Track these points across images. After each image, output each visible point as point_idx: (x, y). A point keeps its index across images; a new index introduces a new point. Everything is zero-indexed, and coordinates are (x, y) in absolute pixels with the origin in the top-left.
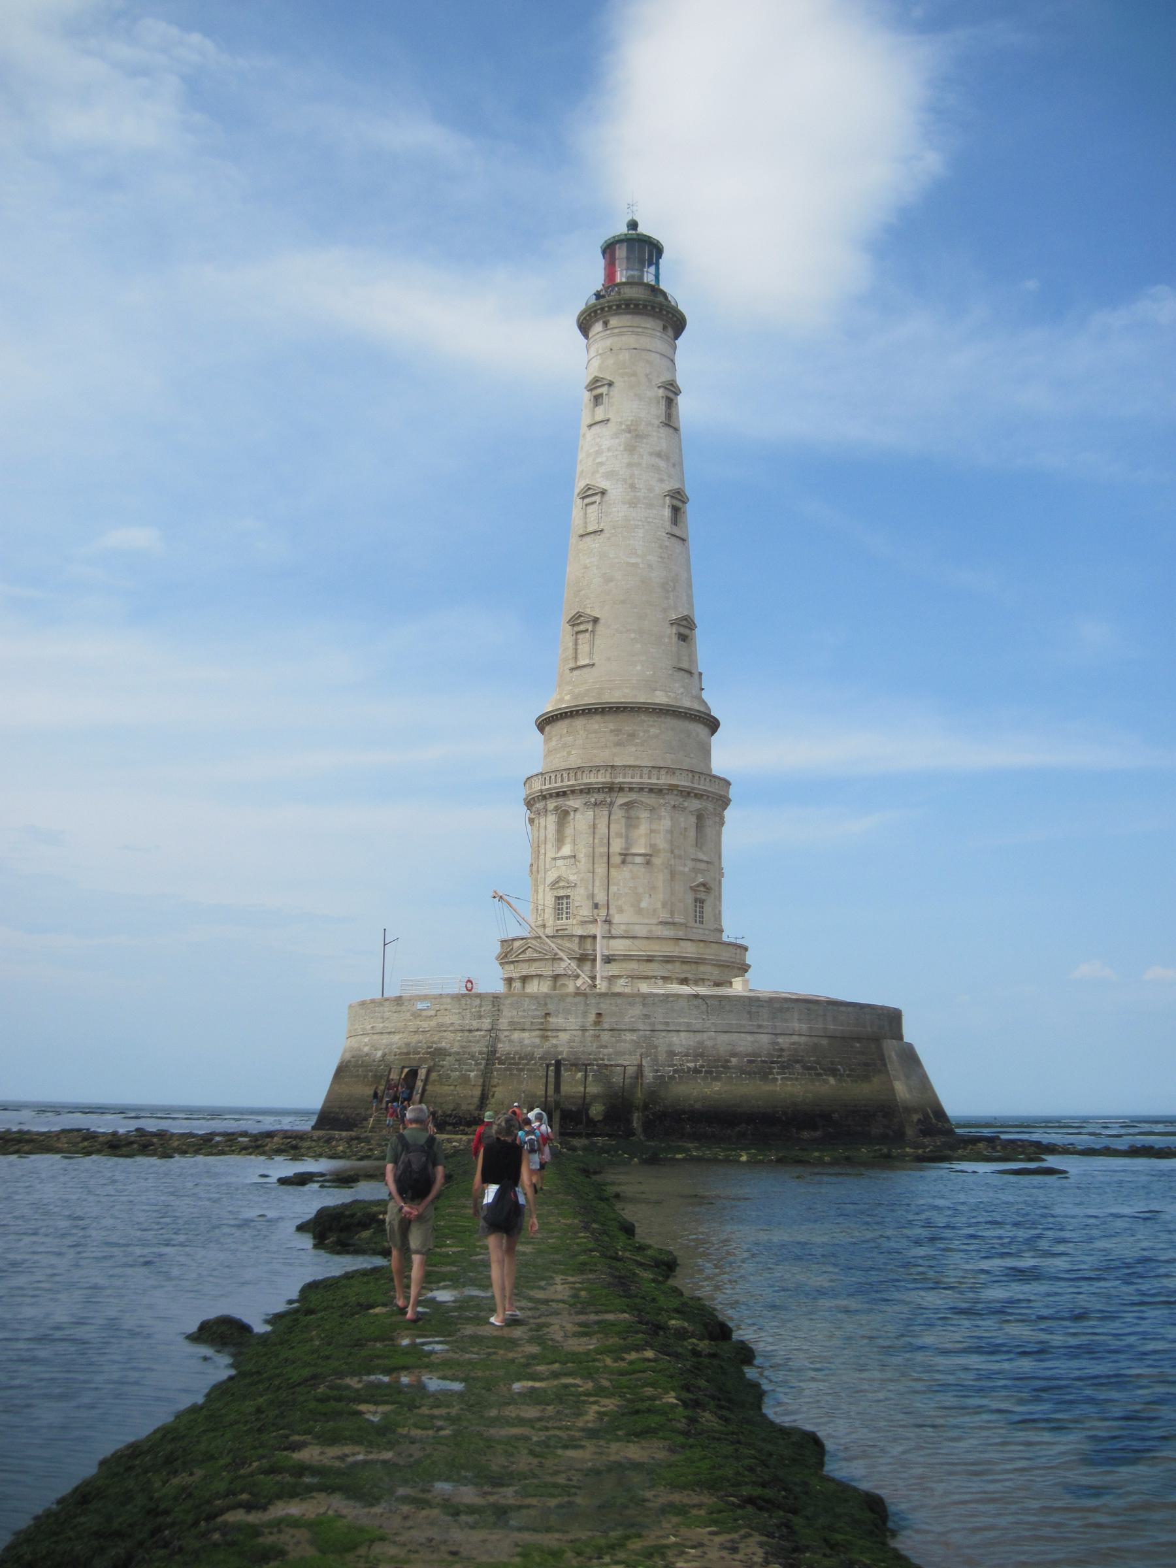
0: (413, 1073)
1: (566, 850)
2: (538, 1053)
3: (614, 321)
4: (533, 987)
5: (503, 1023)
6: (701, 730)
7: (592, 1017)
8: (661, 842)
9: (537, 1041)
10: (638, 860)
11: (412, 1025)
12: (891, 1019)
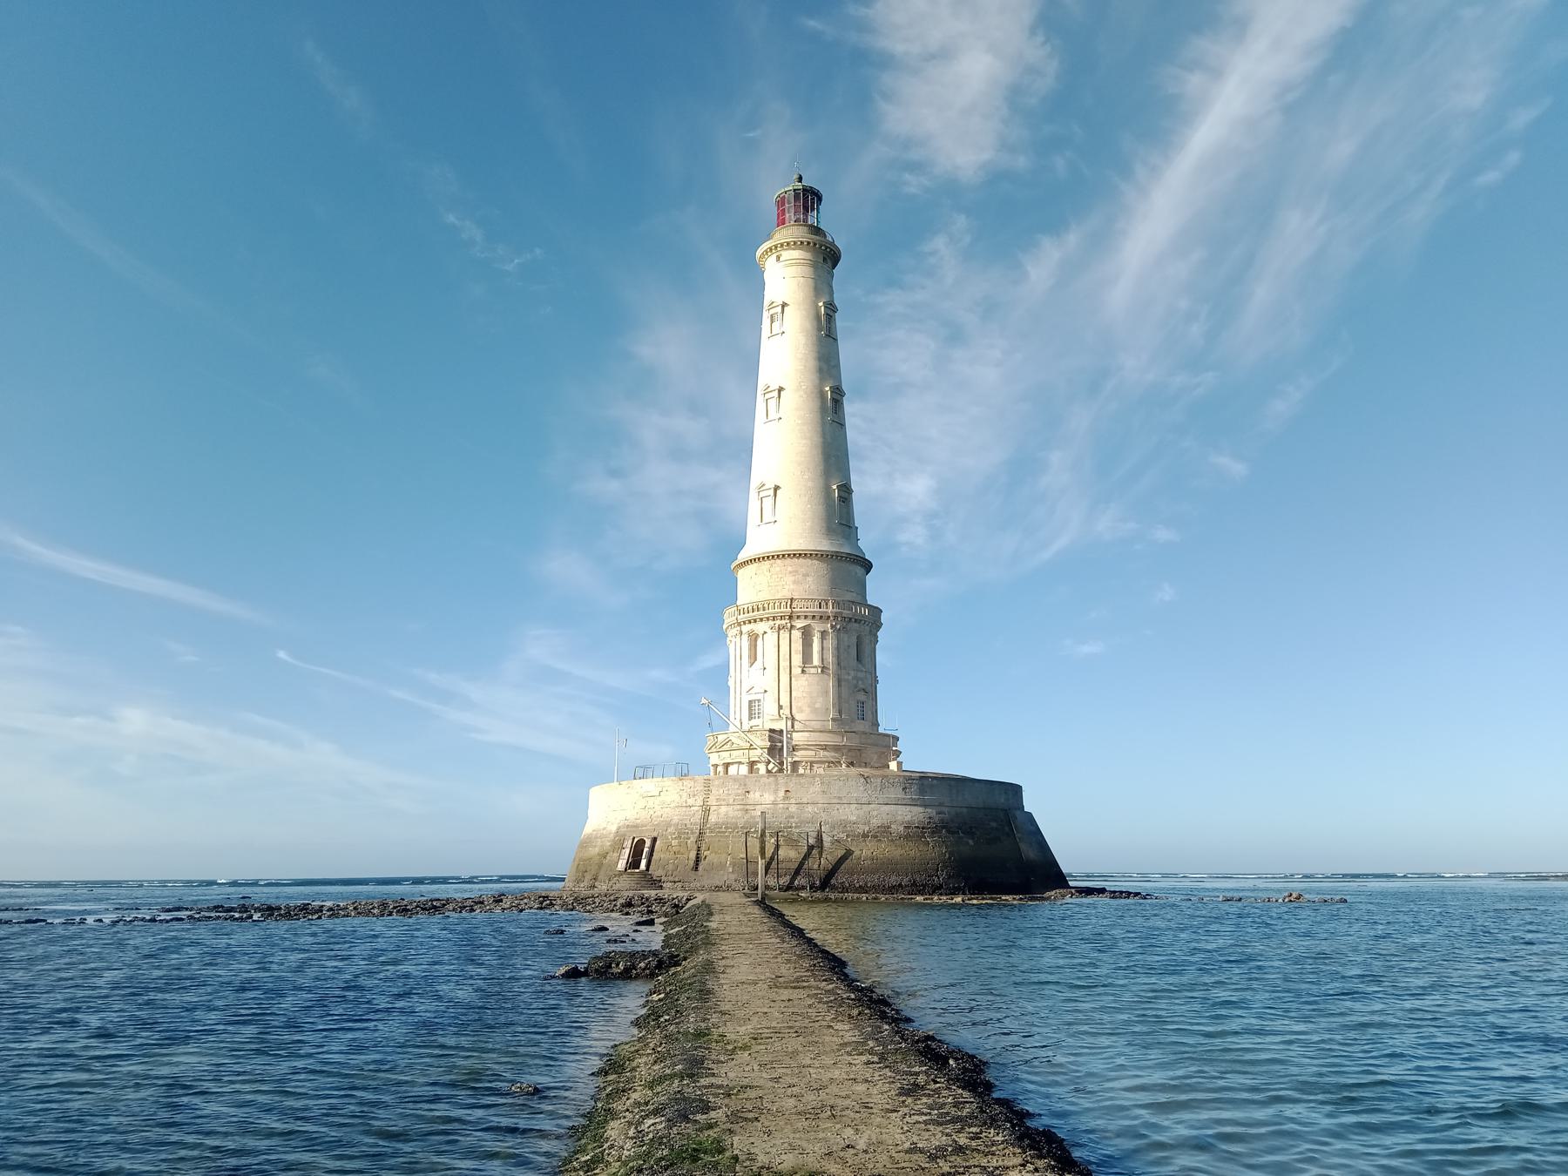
0: (642, 842)
1: (758, 664)
2: (741, 823)
3: (787, 255)
4: (732, 770)
5: (712, 801)
6: (860, 570)
7: (781, 794)
8: (830, 658)
9: (740, 814)
10: (813, 671)
11: (642, 803)
12: (1015, 790)
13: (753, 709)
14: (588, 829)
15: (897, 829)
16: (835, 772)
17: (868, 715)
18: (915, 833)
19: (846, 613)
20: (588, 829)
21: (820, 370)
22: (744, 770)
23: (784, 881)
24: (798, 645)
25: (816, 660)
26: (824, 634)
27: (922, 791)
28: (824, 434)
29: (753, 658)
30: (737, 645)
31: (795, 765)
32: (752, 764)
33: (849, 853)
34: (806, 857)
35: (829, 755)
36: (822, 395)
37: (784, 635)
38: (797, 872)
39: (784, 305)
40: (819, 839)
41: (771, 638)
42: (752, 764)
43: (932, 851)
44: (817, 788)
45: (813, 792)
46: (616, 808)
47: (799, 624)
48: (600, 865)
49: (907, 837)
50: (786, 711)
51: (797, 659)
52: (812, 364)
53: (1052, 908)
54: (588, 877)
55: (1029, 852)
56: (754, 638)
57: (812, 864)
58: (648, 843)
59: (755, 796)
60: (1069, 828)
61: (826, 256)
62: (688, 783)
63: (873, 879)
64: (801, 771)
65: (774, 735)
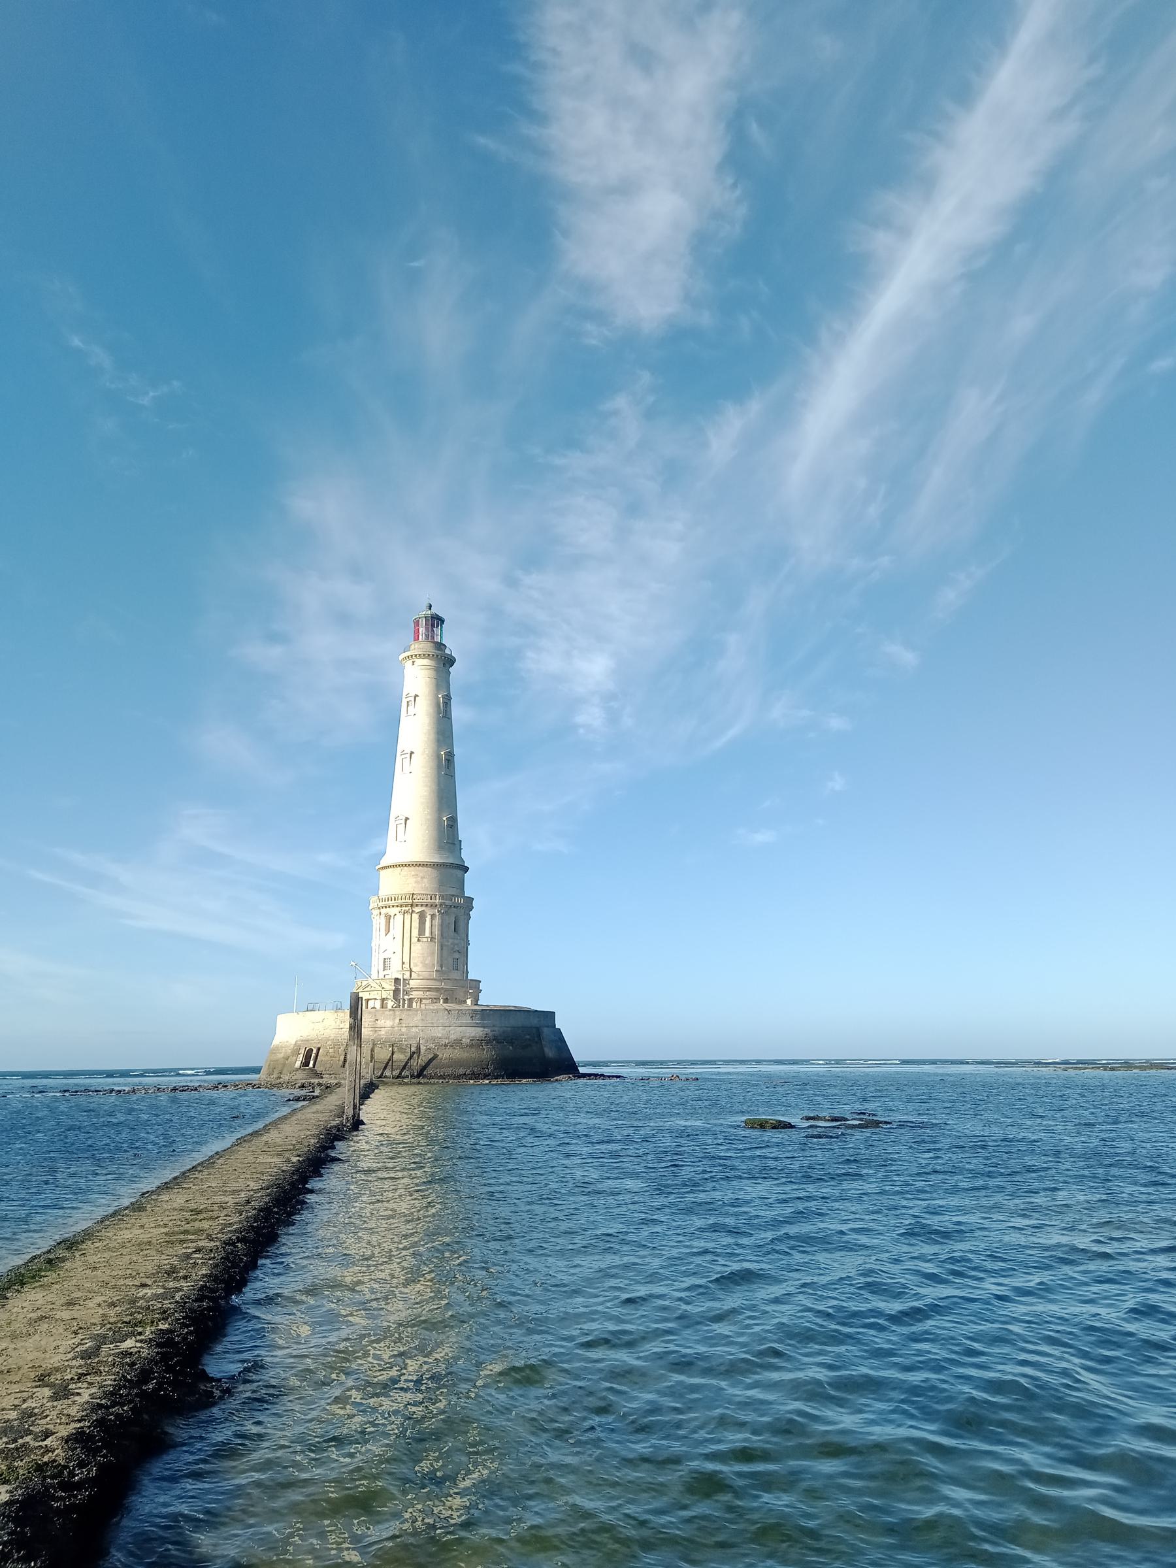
6: (459, 873)
12: (551, 1015)
13: (386, 963)
14: (276, 1042)
15: (466, 1041)
16: (435, 1006)
17: (460, 966)
18: (476, 1043)
19: (448, 902)
20: (276, 1042)
21: (438, 741)
22: (378, 1004)
23: (396, 1073)
24: (416, 923)
25: (427, 934)
26: (433, 916)
27: (482, 1019)
28: (439, 784)
29: (388, 931)
30: (378, 922)
31: (411, 1000)
32: (383, 1000)
33: (436, 1056)
34: (411, 1057)
35: (433, 994)
36: (439, 757)
37: (408, 917)
38: (404, 1068)
39: (416, 696)
40: (419, 1048)
41: (400, 917)
42: (383, 1000)
43: (486, 1053)
44: (419, 1017)
45: (416, 1019)
46: (295, 1029)
47: (417, 909)
48: (284, 1065)
49: (471, 1046)
50: (407, 966)
51: (415, 933)
52: (433, 736)
53: (564, 1088)
54: (276, 1072)
55: (550, 1053)
56: (388, 918)
57: (413, 1062)
58: (315, 1051)
59: (381, 1023)
60: (582, 1040)
61: (444, 662)
62: (341, 1014)
63: (449, 1071)
64: (414, 1004)
65: (397, 980)
